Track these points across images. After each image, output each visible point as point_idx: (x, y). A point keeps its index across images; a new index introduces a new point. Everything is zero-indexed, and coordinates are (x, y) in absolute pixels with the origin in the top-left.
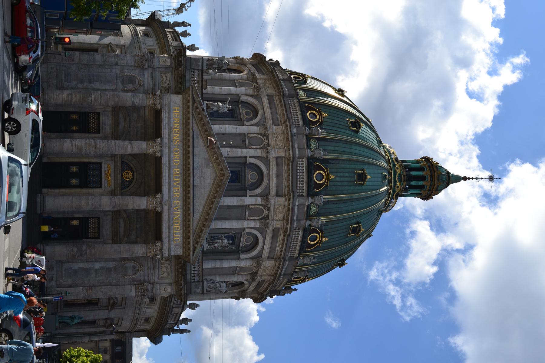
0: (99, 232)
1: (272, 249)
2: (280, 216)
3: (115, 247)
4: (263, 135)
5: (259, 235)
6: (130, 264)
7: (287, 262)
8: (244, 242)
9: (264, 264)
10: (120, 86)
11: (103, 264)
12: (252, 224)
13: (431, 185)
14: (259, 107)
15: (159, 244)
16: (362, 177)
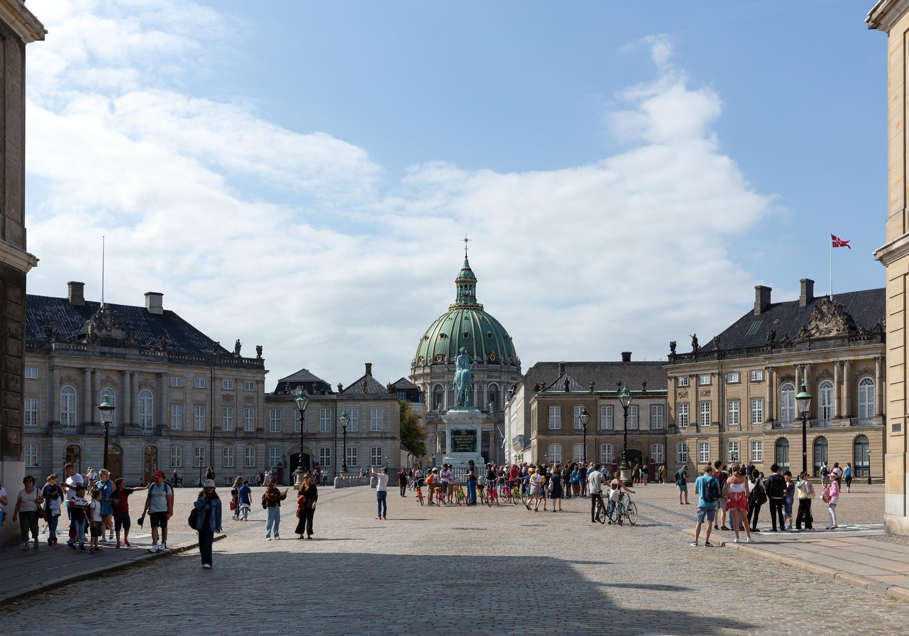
0: (486, 452)
1: (496, 377)
2: (482, 376)
3: (490, 447)
4: (449, 383)
5: (490, 384)
6: (498, 441)
7: (503, 370)
8: (493, 390)
9: (503, 380)
10: (433, 445)
11: (498, 451)
12: (485, 388)
13: (470, 282)
14: (437, 384)
15: (490, 432)
16: (466, 334)
